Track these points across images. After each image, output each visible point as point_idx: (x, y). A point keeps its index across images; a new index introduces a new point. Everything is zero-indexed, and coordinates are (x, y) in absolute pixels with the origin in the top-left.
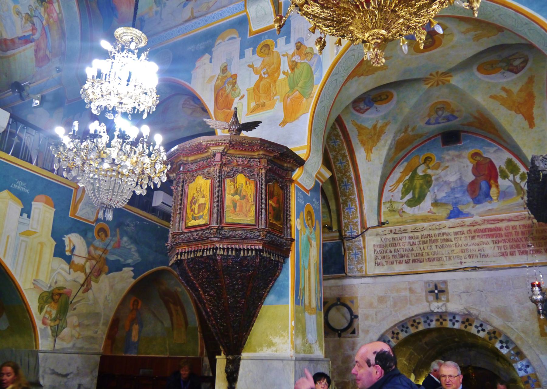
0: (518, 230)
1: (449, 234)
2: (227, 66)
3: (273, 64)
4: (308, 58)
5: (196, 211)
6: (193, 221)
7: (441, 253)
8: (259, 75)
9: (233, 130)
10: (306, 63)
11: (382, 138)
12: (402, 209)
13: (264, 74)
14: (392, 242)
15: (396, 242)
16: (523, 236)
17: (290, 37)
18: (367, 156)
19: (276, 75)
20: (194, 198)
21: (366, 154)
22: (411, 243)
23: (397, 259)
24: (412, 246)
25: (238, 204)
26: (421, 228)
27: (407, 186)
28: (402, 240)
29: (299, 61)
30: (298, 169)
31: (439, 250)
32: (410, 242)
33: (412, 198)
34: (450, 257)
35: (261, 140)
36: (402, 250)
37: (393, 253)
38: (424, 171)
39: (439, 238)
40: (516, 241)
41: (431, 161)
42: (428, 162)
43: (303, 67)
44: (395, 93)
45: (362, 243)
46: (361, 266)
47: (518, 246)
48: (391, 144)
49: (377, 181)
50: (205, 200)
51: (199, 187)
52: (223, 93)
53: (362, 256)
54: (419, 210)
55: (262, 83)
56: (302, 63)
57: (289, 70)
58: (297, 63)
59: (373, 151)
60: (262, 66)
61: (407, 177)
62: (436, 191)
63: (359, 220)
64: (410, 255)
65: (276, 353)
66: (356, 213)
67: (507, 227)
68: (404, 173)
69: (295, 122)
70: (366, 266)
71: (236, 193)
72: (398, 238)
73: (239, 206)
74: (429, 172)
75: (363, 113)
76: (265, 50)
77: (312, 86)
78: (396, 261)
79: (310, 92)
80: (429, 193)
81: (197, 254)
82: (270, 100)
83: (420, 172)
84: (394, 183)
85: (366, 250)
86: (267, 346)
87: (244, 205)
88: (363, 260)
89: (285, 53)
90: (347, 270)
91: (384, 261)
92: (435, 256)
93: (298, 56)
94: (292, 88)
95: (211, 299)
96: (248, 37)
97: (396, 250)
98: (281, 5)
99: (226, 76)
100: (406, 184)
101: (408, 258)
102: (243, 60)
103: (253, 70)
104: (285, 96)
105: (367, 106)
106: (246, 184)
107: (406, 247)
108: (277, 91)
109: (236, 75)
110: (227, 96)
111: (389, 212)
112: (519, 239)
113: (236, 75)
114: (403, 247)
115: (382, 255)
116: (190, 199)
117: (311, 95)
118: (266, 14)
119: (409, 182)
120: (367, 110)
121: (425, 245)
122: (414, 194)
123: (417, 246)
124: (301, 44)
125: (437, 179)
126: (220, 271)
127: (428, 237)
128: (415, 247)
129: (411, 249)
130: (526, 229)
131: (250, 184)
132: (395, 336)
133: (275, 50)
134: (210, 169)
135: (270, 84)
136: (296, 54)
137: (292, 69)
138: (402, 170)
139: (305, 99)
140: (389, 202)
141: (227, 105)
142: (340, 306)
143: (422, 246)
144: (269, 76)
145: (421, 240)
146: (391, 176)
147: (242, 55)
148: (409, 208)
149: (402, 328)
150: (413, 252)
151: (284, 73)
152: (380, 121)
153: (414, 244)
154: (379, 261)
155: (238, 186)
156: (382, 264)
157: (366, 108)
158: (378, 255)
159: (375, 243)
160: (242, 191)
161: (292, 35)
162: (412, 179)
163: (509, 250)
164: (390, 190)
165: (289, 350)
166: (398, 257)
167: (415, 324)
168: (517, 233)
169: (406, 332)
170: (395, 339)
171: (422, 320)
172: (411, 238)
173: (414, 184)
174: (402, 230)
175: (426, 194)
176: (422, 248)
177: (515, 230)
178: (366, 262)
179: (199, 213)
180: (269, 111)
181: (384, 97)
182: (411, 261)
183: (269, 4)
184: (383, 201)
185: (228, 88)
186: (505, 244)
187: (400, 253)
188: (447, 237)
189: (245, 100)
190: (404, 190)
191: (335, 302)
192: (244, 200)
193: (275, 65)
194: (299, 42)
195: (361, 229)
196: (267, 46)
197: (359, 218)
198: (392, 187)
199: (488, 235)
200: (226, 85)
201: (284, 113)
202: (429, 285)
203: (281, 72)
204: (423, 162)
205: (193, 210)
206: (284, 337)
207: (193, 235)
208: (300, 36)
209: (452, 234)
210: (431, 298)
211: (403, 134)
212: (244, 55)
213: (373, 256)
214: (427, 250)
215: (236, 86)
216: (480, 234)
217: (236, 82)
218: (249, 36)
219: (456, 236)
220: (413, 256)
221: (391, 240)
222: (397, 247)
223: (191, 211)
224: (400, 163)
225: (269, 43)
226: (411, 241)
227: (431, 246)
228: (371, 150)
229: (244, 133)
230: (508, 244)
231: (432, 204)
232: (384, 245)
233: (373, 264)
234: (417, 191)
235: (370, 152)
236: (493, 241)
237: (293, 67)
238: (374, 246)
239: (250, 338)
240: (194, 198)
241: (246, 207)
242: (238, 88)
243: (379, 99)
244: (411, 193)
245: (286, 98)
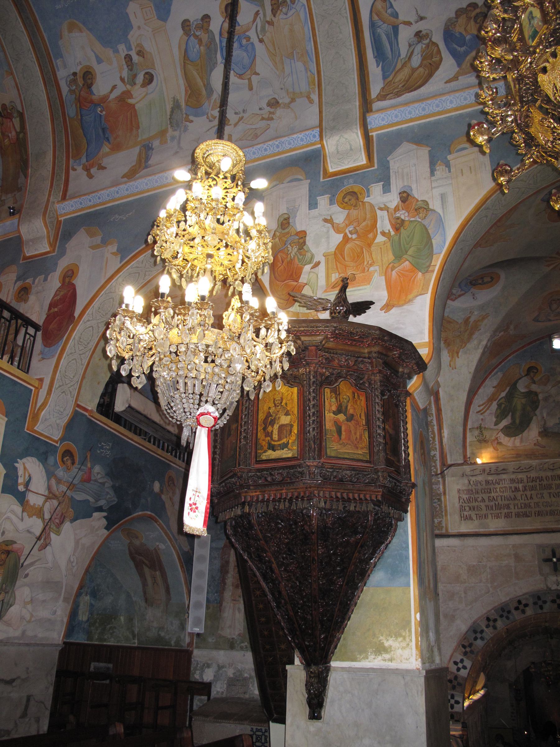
2: (289, 218)
3: (364, 221)
4: (421, 215)
5: (275, 437)
6: (270, 452)
8: (343, 235)
9: (339, 313)
10: (419, 222)
11: (474, 336)
12: (497, 438)
13: (351, 232)
15: (492, 487)
17: (390, 185)
18: (450, 361)
19: (371, 236)
20: (269, 415)
21: (449, 359)
23: (492, 512)
25: (343, 429)
26: (527, 467)
27: (503, 406)
29: (407, 219)
30: (415, 378)
31: (554, 499)
32: (511, 488)
33: (511, 424)
35: (380, 329)
36: (500, 497)
37: (487, 503)
38: (526, 387)
41: (536, 373)
42: (532, 374)
43: (415, 227)
44: (503, 275)
45: (441, 487)
46: (439, 520)
48: (486, 345)
49: (463, 397)
50: (291, 420)
51: (278, 398)
52: (285, 256)
54: (521, 441)
55: (348, 246)
56: (411, 221)
57: (391, 230)
58: (403, 221)
59: (460, 354)
60: (347, 222)
61: (503, 394)
62: (545, 415)
63: (438, 454)
64: (512, 506)
65: (390, 663)
66: (433, 443)
68: (499, 387)
69: (405, 307)
70: (447, 520)
71: (339, 411)
72: (494, 481)
73: (345, 431)
74: (534, 387)
75: (454, 300)
76: (350, 200)
77: (431, 255)
78: (492, 514)
79: (428, 264)
80: (534, 418)
81: (279, 506)
82: (363, 271)
83: (522, 387)
84: (484, 402)
85: (447, 497)
86: (375, 652)
87: (352, 428)
89: (383, 206)
92: (548, 509)
93: (404, 212)
94: (399, 256)
95: (289, 576)
96: (322, 180)
97: (491, 498)
98: (373, 140)
99: (288, 233)
101: (509, 511)
102: (315, 212)
103: (333, 227)
104: (387, 267)
105: (462, 290)
106: (354, 397)
107: (505, 494)
108: (374, 260)
109: (304, 232)
110: (291, 262)
113: (304, 232)
114: (501, 494)
115: (471, 505)
116: (261, 416)
117: (431, 269)
118: (351, 149)
120: (460, 296)
121: (533, 492)
122: (513, 418)
124: (408, 195)
125: (546, 399)
126: (313, 533)
127: (538, 480)
128: (518, 495)
129: (512, 497)
131: (358, 396)
132: (491, 623)
133: (366, 200)
134: (298, 371)
135: (362, 249)
136: (400, 208)
137: (397, 230)
138: (495, 383)
139: (420, 274)
140: (477, 428)
141: (292, 275)
143: (528, 493)
144: (359, 237)
146: (481, 391)
147: (313, 205)
148: (507, 439)
149: (501, 613)
150: (516, 502)
151: (383, 234)
152: (476, 313)
154: (465, 513)
155: (342, 400)
156: (471, 518)
157: (459, 293)
159: (459, 487)
160: (349, 408)
161: (393, 180)
162: (510, 397)
165: (413, 659)
167: (521, 607)
169: (508, 618)
170: (491, 628)
172: (512, 481)
174: (499, 469)
175: (532, 419)
176: (529, 497)
178: (446, 515)
179: (280, 439)
180: (361, 288)
181: (486, 280)
182: (513, 514)
183: (358, 136)
184: (469, 426)
185: (293, 251)
187: (497, 503)
189: (322, 270)
190: (499, 411)
192: (353, 422)
193: (368, 222)
194: (404, 192)
195: (441, 466)
196: (354, 194)
197: (438, 450)
198: (482, 408)
200: (289, 246)
201: (388, 292)
203: (379, 233)
204: (526, 373)
205: (270, 435)
206: (404, 638)
207: (271, 474)
208: (406, 184)
210: (547, 569)
211: (502, 333)
212: (316, 204)
213: (457, 505)
215: (305, 247)
217: (304, 243)
218: (324, 178)
220: (516, 507)
221: (484, 483)
223: (266, 436)
224: (493, 374)
225: (356, 190)
226: (513, 485)
227: (542, 494)
228: (458, 353)
229: (351, 319)
231: (539, 432)
232: (474, 491)
233: (457, 517)
234: (518, 414)
235: (455, 355)
237: (398, 225)
238: (459, 491)
239: (344, 639)
240: (271, 416)
241: (355, 434)
242: (309, 251)
243: (480, 282)
244: (509, 417)
245: (390, 270)
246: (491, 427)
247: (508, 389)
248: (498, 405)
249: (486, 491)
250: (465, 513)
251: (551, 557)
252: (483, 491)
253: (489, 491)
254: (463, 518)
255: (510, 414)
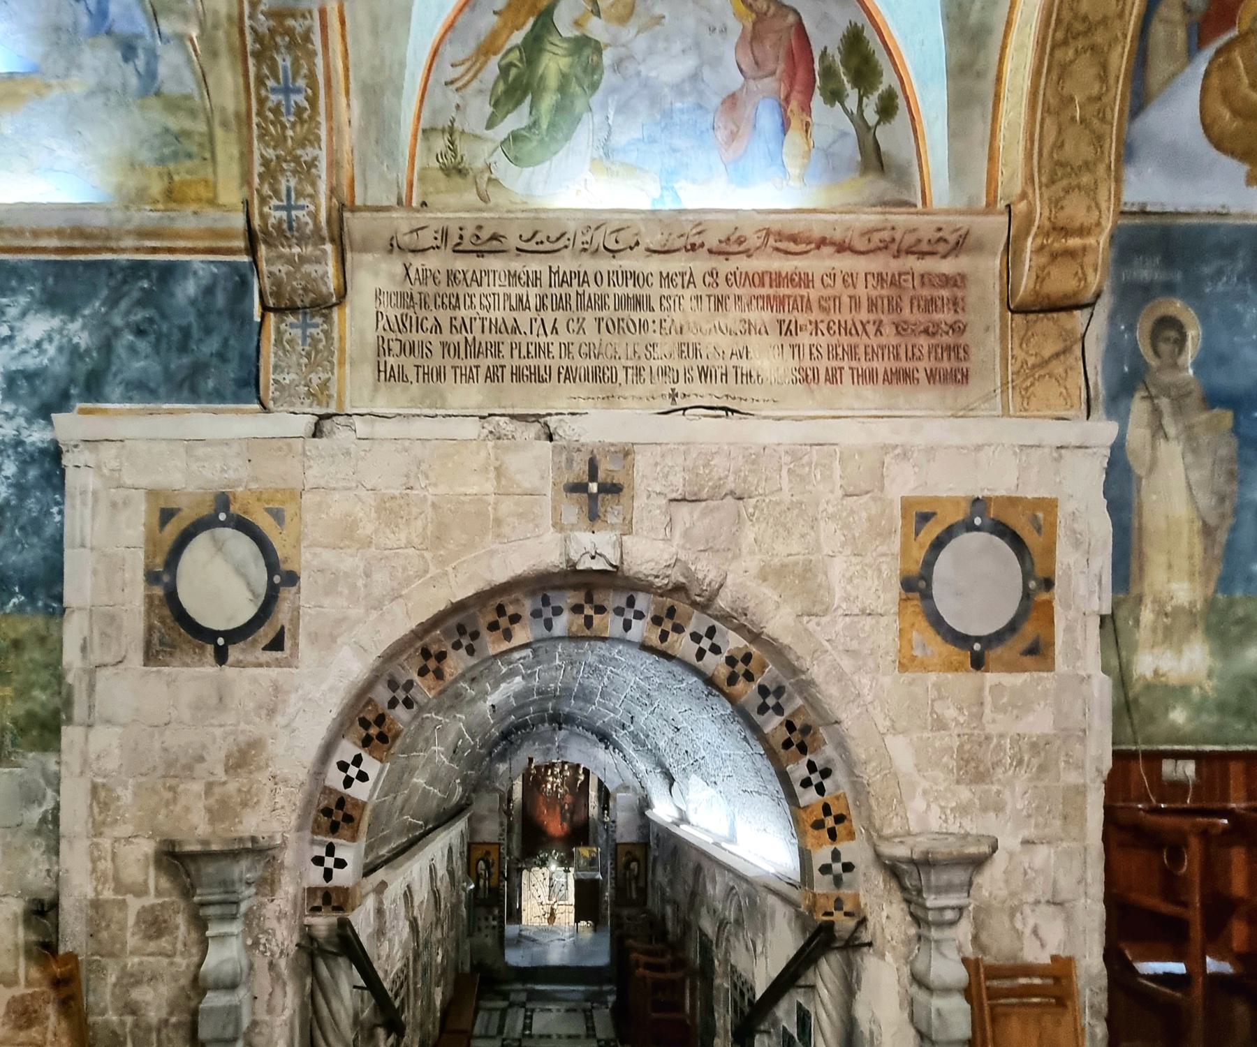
0: (861, 291)
1: (646, 280)
7: (610, 351)
14: (443, 288)
15: (461, 290)
16: (872, 317)
22: (514, 304)
23: (457, 362)
24: (515, 314)
28: (480, 285)
34: (639, 371)
36: (479, 322)
37: (447, 336)
38: (577, 24)
39: (613, 290)
40: (848, 332)
47: (852, 352)
53: (327, 334)
64: (505, 350)
67: (829, 276)
72: (469, 276)
88: (332, 353)
90: (267, 388)
91: (408, 362)
97: (458, 323)
100: (511, 65)
101: (498, 362)
107: (493, 315)
111: (441, 175)
112: (860, 328)
114: (483, 313)
119: (521, 60)
121: (560, 315)
123: (533, 314)
127: (575, 282)
128: (523, 318)
129: (510, 324)
130: (885, 292)
142: (229, 532)
143: (549, 316)
145: (550, 291)
150: (517, 338)
153: (522, 304)
154: (391, 361)
158: (393, 336)
163: (823, 364)
164: (452, 82)
166: (462, 355)
168: (855, 302)
171: (527, 606)
172: (513, 277)
173: (540, 72)
177: (851, 291)
178: (342, 363)
186: (814, 340)
188: (638, 291)
190: (501, 87)
191: (206, 511)
199: (768, 297)
202: (570, 461)
209: (655, 280)
210: (572, 511)
213: (371, 337)
214: (564, 337)
216: (745, 291)
219: (666, 292)
220: (516, 352)
221: (443, 277)
222: (463, 313)
230: (823, 341)
232: (416, 297)
236: (781, 322)
246: (478, 132)
247: (531, 21)
248: (500, 67)
249: (446, 301)
250: (391, 361)
251: (586, 478)
252: (439, 301)
253: (453, 301)
254: (382, 374)
255: (529, 98)
